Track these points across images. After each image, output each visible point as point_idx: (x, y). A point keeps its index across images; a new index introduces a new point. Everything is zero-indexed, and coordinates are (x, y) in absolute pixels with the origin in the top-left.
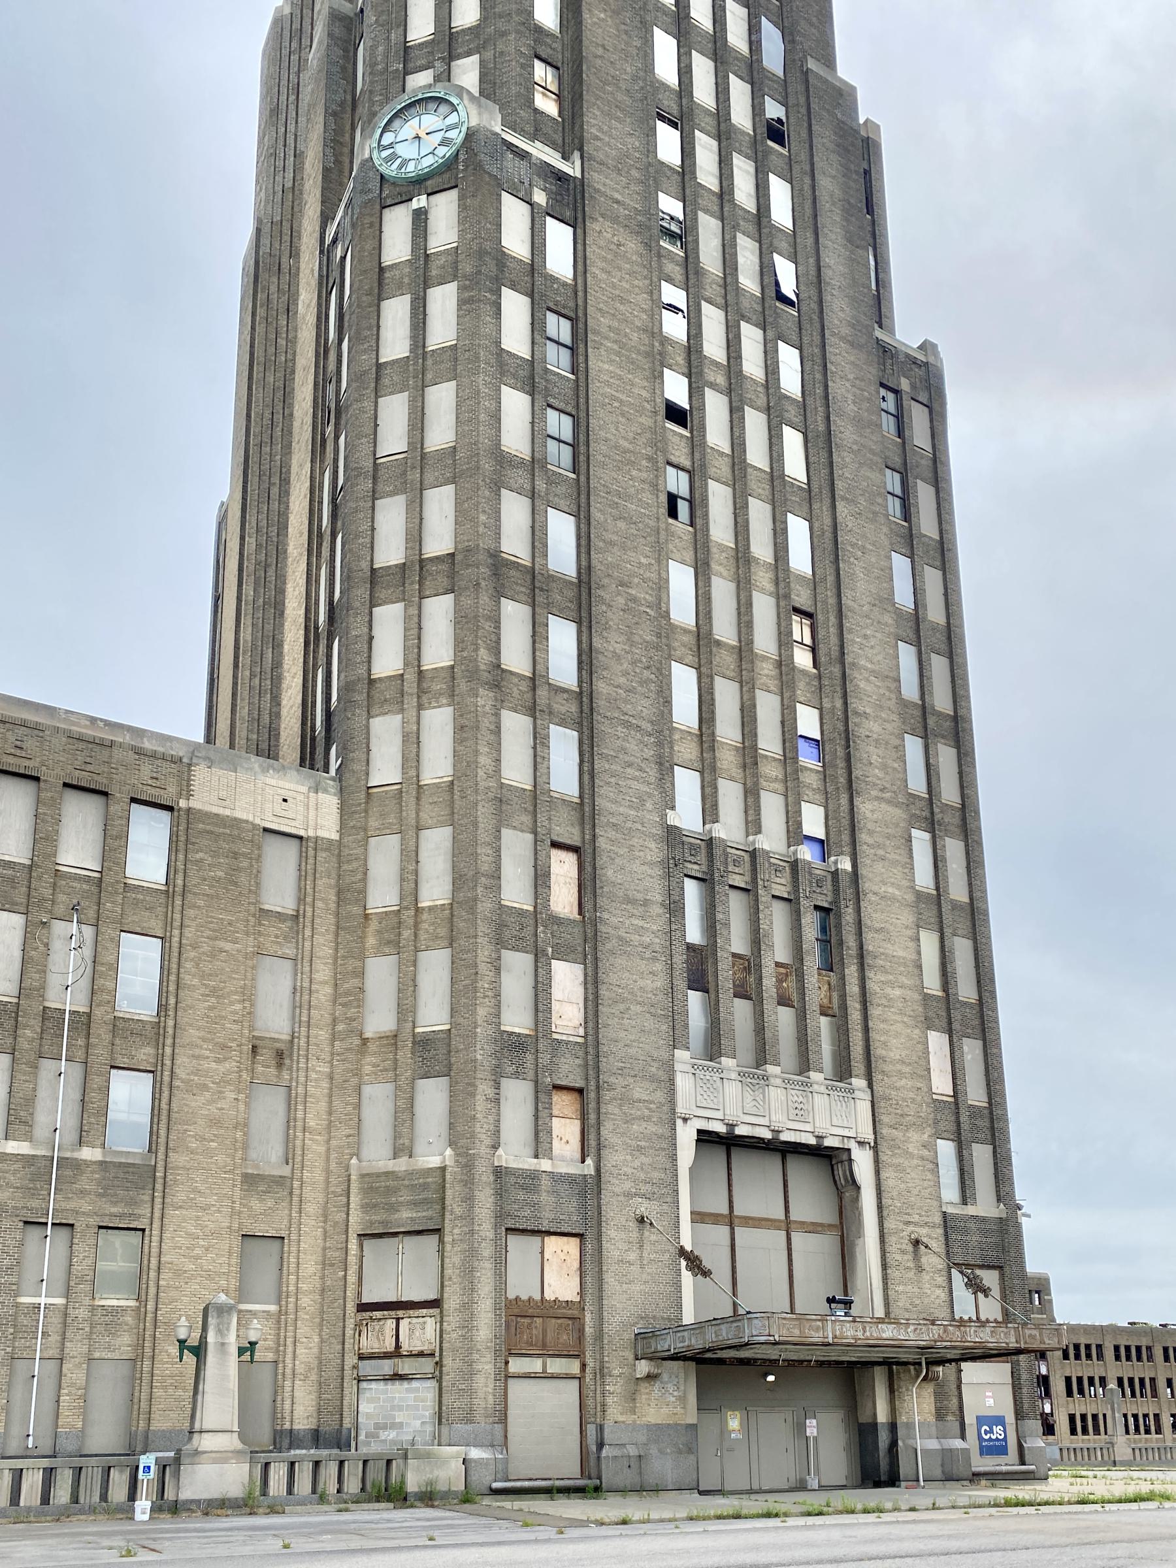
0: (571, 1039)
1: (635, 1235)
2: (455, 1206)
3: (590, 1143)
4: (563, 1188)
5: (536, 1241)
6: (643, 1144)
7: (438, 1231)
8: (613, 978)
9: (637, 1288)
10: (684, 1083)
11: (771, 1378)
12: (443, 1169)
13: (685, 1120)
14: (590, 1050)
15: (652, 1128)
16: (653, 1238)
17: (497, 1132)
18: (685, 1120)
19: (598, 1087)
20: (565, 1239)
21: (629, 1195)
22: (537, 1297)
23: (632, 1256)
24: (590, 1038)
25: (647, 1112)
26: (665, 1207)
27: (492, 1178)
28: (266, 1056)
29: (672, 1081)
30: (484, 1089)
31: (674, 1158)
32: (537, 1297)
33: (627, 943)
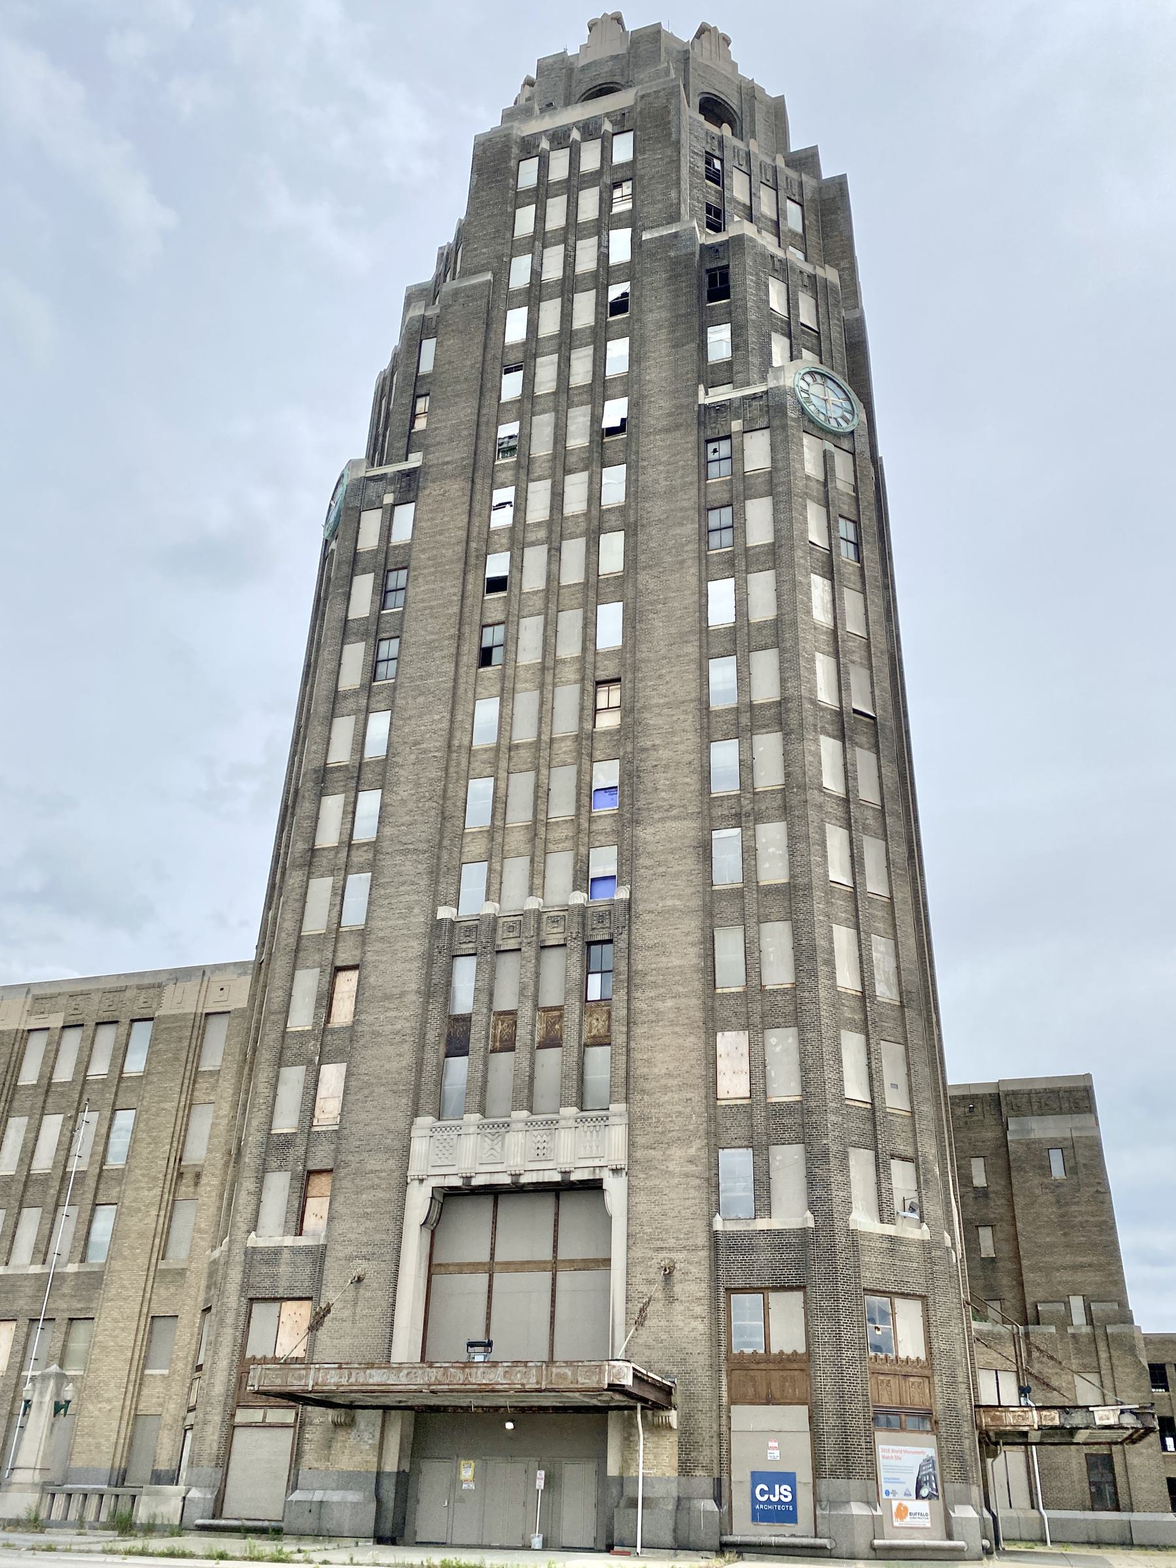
0: (330, 1128)
1: (350, 1294)
4: (300, 1259)
6: (368, 1210)
8: (363, 1069)
9: (348, 1341)
10: (419, 1147)
11: (509, 1426)
13: (421, 1181)
15: (381, 1194)
16: (368, 1294)
21: (350, 1258)
25: (377, 1181)
26: (383, 1265)
28: (188, 1179)
29: (407, 1149)
31: (400, 1220)
33: (379, 1034)
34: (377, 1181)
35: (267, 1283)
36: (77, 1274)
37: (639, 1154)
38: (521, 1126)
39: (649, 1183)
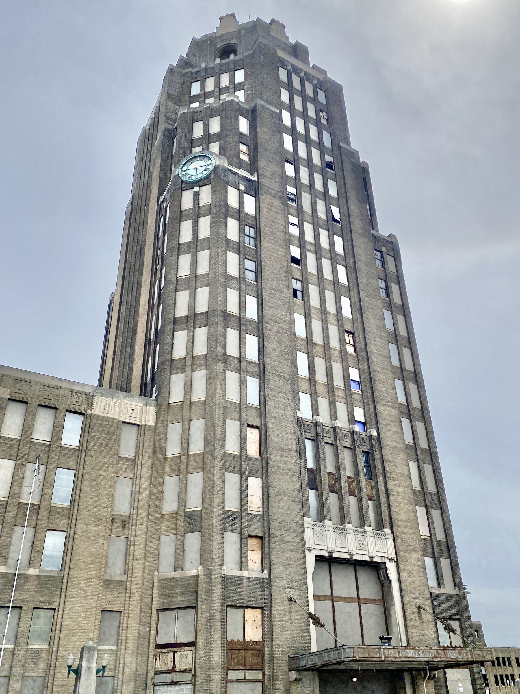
0: (257, 513)
1: (287, 608)
2: (203, 594)
3: (266, 562)
5: (241, 610)
7: (195, 607)
10: (308, 533)
11: (355, 679)
12: (197, 577)
13: (309, 550)
14: (266, 518)
16: (296, 608)
17: (223, 558)
18: (309, 550)
19: (269, 536)
20: (255, 610)
21: (284, 588)
22: (242, 640)
23: (287, 618)
24: (265, 512)
25: (292, 547)
27: (220, 581)
29: (303, 532)
30: (217, 537)
31: (305, 569)
32: (242, 640)
33: (282, 469)
34: (292, 547)
35: (237, 597)
36: (38, 576)
37: (401, 553)
38: (351, 531)
39: (406, 568)
